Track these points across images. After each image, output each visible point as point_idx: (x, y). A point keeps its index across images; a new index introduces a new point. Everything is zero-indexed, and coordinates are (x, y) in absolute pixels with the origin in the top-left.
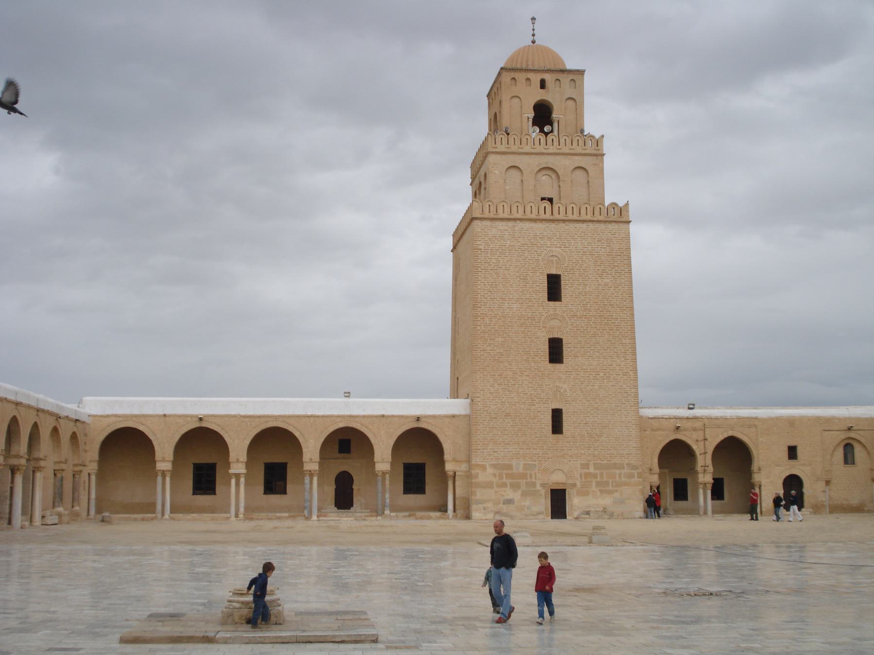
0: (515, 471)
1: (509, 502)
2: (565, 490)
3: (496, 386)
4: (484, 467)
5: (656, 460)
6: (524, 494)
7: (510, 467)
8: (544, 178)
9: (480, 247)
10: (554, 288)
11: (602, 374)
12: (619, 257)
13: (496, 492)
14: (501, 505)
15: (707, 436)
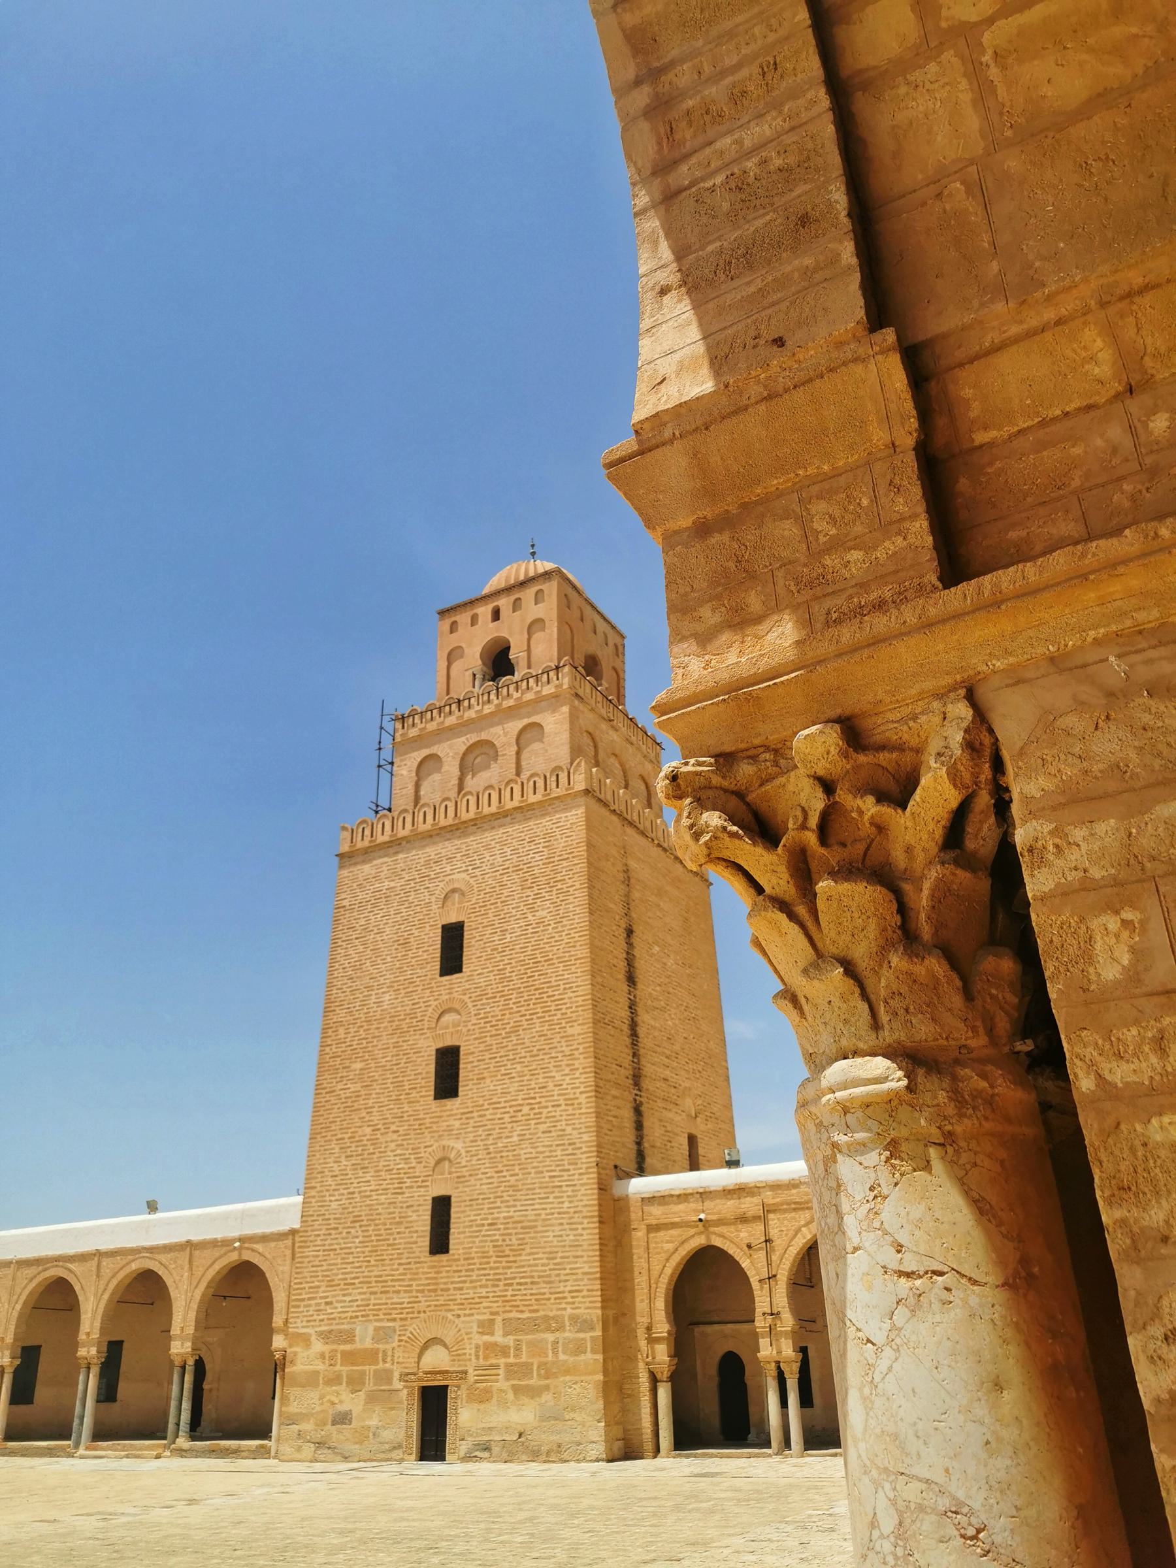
0: (358, 1345)
1: (342, 1419)
2: (445, 1388)
3: (343, 1159)
4: (305, 1340)
5: (660, 1303)
6: (371, 1399)
7: (349, 1337)
8: (479, 760)
9: (346, 903)
10: (452, 950)
11: (526, 1109)
12: (565, 864)
13: (322, 1397)
14: (329, 1427)
15: (774, 1233)
